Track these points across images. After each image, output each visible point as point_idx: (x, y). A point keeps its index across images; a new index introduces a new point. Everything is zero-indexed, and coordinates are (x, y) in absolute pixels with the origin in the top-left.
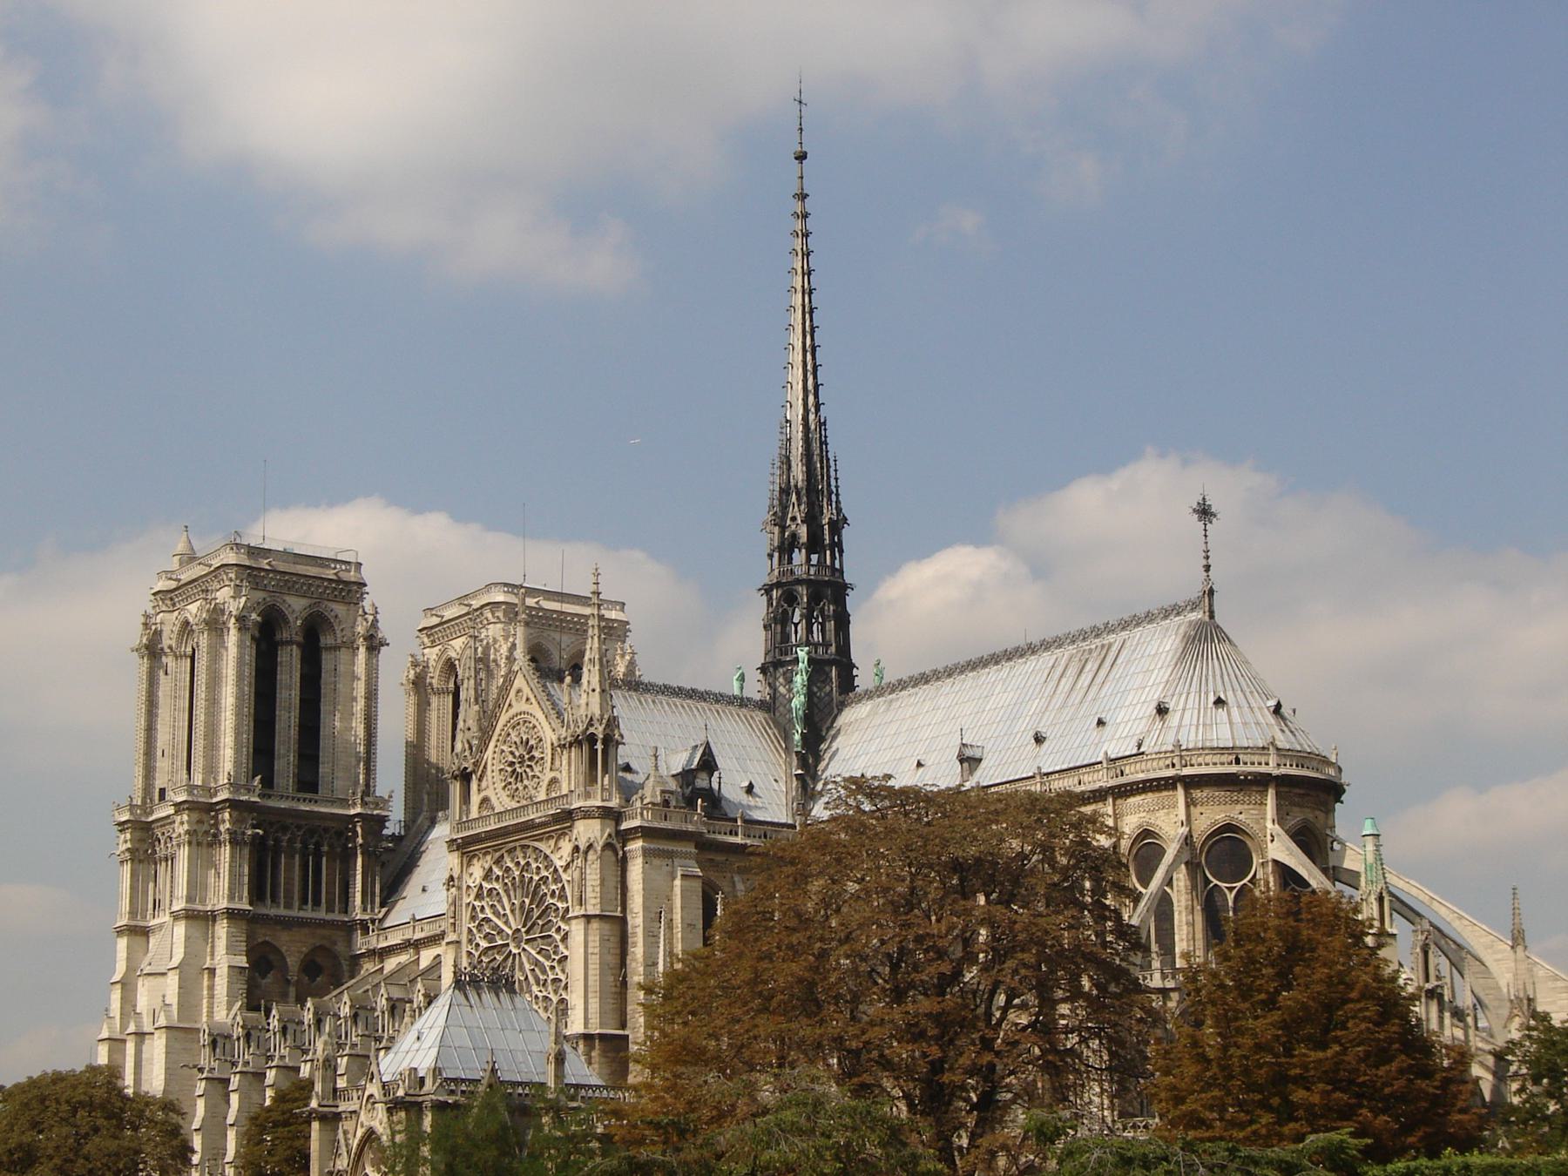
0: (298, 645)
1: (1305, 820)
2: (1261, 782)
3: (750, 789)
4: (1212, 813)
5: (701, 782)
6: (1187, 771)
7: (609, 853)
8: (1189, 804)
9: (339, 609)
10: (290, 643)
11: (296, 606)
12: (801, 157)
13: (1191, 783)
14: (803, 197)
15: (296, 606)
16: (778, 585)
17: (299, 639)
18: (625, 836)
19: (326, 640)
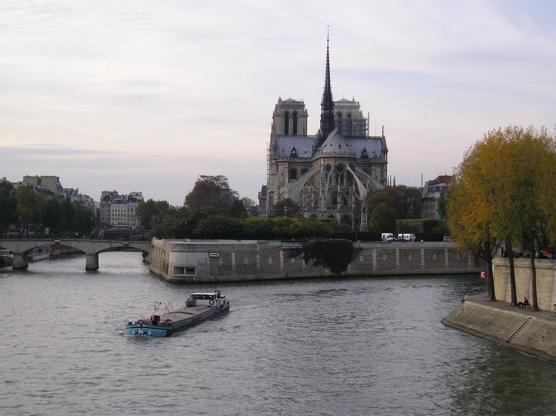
0: (292, 117)
1: (340, 164)
2: (332, 157)
3: (306, 152)
4: (326, 163)
5: (294, 152)
6: (323, 156)
7: (275, 165)
8: (324, 161)
9: (299, 110)
10: (290, 117)
11: (291, 111)
12: (328, 40)
13: (324, 158)
14: (328, 48)
15: (291, 111)
16: (321, 116)
17: (293, 116)
18: (278, 162)
19: (298, 116)
